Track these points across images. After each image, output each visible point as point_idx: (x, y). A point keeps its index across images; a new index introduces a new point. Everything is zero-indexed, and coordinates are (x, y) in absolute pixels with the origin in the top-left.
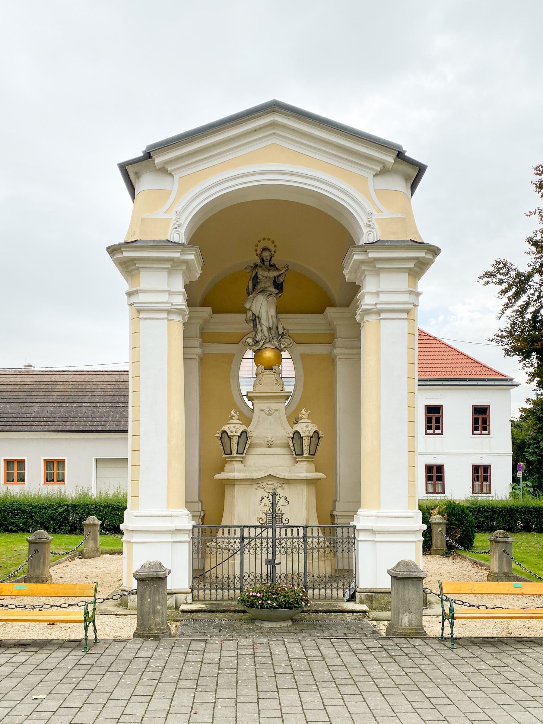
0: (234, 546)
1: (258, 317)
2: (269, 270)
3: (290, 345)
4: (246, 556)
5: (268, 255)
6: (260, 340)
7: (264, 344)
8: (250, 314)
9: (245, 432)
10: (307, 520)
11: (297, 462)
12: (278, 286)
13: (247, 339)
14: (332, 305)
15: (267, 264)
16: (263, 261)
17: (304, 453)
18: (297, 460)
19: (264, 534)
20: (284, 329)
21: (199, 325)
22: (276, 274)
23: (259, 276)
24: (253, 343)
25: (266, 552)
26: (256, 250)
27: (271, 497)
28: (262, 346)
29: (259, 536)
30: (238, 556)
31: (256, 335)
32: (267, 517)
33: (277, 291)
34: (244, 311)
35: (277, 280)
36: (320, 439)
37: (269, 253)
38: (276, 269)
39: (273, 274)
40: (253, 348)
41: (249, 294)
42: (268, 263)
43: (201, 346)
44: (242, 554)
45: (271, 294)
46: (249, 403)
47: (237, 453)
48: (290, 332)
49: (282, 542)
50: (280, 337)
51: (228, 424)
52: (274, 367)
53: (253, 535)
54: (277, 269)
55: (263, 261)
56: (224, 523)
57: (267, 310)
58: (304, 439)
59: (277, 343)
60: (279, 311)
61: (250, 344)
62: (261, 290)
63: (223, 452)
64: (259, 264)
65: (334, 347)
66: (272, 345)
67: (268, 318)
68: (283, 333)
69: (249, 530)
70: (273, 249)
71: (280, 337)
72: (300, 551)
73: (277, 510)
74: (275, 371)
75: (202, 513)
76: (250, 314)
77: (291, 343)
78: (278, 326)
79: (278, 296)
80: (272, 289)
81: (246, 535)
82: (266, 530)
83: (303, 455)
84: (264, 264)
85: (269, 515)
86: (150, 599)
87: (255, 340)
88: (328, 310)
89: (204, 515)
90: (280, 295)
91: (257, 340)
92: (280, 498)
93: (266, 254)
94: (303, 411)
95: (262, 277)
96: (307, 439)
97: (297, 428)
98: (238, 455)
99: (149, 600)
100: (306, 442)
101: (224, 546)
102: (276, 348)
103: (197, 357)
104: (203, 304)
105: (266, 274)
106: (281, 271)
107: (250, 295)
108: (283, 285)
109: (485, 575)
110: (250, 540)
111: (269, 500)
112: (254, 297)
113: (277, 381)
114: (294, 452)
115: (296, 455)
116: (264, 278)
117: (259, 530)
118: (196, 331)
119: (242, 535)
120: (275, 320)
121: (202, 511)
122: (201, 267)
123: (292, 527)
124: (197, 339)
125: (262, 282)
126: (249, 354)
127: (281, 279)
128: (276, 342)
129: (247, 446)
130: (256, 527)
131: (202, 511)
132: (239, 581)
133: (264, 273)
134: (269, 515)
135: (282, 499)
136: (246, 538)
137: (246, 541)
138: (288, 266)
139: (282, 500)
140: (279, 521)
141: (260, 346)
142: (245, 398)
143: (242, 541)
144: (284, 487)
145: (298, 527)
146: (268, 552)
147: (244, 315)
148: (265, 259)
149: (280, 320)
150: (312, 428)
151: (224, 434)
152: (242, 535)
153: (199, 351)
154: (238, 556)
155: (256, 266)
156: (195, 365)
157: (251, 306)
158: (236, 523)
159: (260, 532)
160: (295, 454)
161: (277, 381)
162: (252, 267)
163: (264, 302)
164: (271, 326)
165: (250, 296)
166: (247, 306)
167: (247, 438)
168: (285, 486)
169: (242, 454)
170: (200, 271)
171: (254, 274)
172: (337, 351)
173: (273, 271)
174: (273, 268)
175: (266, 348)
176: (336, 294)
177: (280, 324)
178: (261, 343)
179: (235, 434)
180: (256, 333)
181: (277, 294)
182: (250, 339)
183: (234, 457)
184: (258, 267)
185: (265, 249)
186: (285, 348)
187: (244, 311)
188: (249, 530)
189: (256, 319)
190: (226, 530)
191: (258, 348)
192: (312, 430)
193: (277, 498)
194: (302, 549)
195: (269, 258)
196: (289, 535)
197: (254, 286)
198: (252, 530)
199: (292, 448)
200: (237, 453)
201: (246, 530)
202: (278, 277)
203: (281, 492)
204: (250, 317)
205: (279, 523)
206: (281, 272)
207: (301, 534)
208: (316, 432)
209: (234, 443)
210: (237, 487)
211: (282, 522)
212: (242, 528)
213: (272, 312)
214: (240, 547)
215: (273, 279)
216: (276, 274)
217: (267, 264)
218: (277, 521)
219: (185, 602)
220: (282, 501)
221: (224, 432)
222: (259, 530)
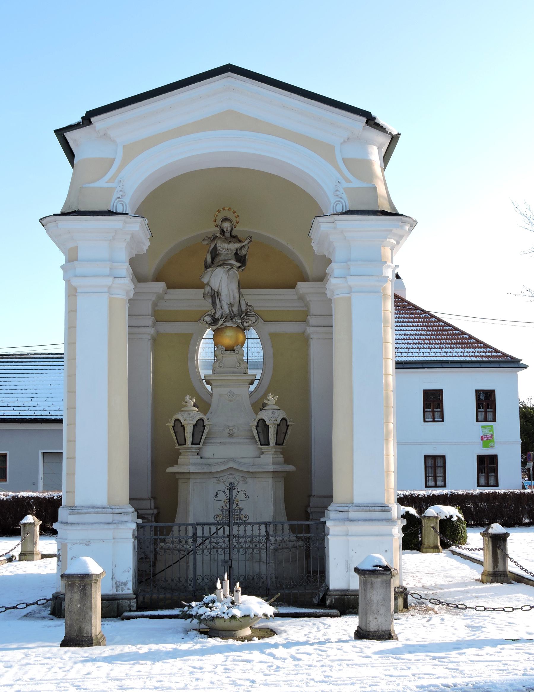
0: (185, 546)
1: (218, 293)
2: (229, 241)
3: (255, 324)
4: (199, 557)
5: (229, 226)
6: (220, 318)
7: (224, 322)
8: (208, 289)
9: (202, 420)
10: (274, 517)
11: (263, 453)
12: (241, 259)
13: (205, 316)
14: (305, 279)
15: (228, 235)
16: (223, 232)
17: (270, 443)
18: (262, 451)
19: (221, 532)
20: (247, 305)
21: (151, 302)
22: (237, 245)
23: (219, 248)
24: (212, 321)
25: (223, 552)
26: (215, 221)
27: (227, 492)
28: (222, 325)
29: (215, 535)
30: (191, 557)
31: (215, 312)
32: (223, 514)
33: (238, 264)
34: (202, 286)
35: (239, 253)
36: (289, 427)
37: (230, 224)
38: (237, 241)
39: (234, 246)
40: (211, 326)
41: (207, 267)
42: (229, 234)
43: (154, 325)
44: (195, 554)
45: (232, 268)
46: (209, 388)
47: (193, 444)
48: (255, 309)
49: (240, 541)
50: (244, 314)
51: (182, 411)
52: (235, 348)
53: (206, 534)
54: (240, 241)
55: (223, 232)
56: (178, 520)
57: (228, 286)
58: (269, 427)
59: (239, 321)
60: (241, 286)
61: (209, 323)
62: (220, 263)
63: (176, 442)
64: (218, 235)
65: (308, 325)
66: (234, 323)
67: (229, 293)
68: (246, 310)
69: (203, 528)
70: (234, 219)
71: (244, 314)
72: (262, 551)
73: (235, 505)
74: (237, 352)
75: (155, 511)
76: (208, 289)
77: (256, 321)
78: (241, 301)
79: (240, 270)
80: (233, 262)
81: (199, 533)
82: (222, 529)
83: (269, 445)
84: (224, 235)
85: (226, 512)
86: (81, 604)
87: (214, 318)
88: (300, 285)
89: (158, 513)
90: (243, 268)
91: (216, 317)
92: (238, 492)
93: (227, 225)
94: (270, 396)
95: (221, 249)
96: (273, 428)
97: (263, 415)
98: (194, 446)
99: (79, 606)
100: (272, 431)
101: (174, 546)
102: (238, 326)
103: (149, 337)
104: (157, 279)
105: (226, 246)
106: (243, 242)
107: (208, 268)
108: (247, 258)
109: (256, 566)
110: (204, 539)
111: (226, 495)
112: (213, 271)
113: (240, 364)
114: (258, 442)
115: (261, 445)
116: (224, 250)
117: (213, 528)
118: (148, 309)
119: (195, 534)
120: (237, 295)
121: (155, 508)
122: (149, 238)
123: (252, 524)
124: (149, 317)
125: (222, 254)
126: (209, 333)
127: (244, 252)
128: (238, 319)
129: (204, 436)
130: (210, 524)
131: (155, 508)
132: (192, 585)
133: (224, 244)
134: (226, 512)
135: (241, 493)
136: (200, 537)
137: (199, 541)
138: (251, 238)
139: (241, 493)
140: (237, 518)
141: (219, 325)
142: (204, 381)
143: (195, 540)
144: (247, 481)
145: (259, 524)
146: (224, 552)
147: (201, 291)
148: (225, 230)
149: (243, 296)
150: (280, 415)
151: (177, 422)
152: (195, 534)
153: (152, 331)
154: (191, 557)
155: (215, 238)
156: (146, 347)
157: (209, 281)
158: (191, 520)
159: (219, 532)
160: (260, 445)
161: (240, 364)
162: (210, 238)
163: (225, 277)
164: (232, 302)
165: (208, 270)
166: (205, 280)
167: (204, 426)
168: (249, 480)
169: (199, 444)
170: (148, 243)
171: (212, 246)
172: (310, 330)
173: (234, 243)
174: (235, 239)
175: (227, 327)
176: (310, 269)
177: (243, 301)
178: (221, 322)
179: (190, 422)
180: (215, 310)
181: (239, 267)
182: (208, 316)
183: (188, 448)
184: (217, 239)
185: (225, 220)
186: (248, 326)
187: (202, 286)
188: (203, 528)
189: (215, 296)
190: (183, 528)
191: (217, 326)
192: (279, 418)
193: (235, 492)
194: (263, 549)
195: (229, 229)
196: (249, 533)
197: (213, 259)
198: (206, 528)
199: (257, 437)
200: (193, 444)
201: (199, 528)
202: (241, 248)
203: (240, 487)
204: (208, 293)
205: (237, 520)
206: (243, 244)
207: (263, 532)
208: (283, 419)
209: (188, 433)
210: (192, 481)
211: (240, 519)
212: (195, 526)
213: (234, 286)
214: (192, 547)
215: (235, 251)
216: (237, 245)
217: (228, 235)
218: (234, 518)
219: (129, 609)
220: (241, 496)
221: (177, 420)
222: (213, 528)
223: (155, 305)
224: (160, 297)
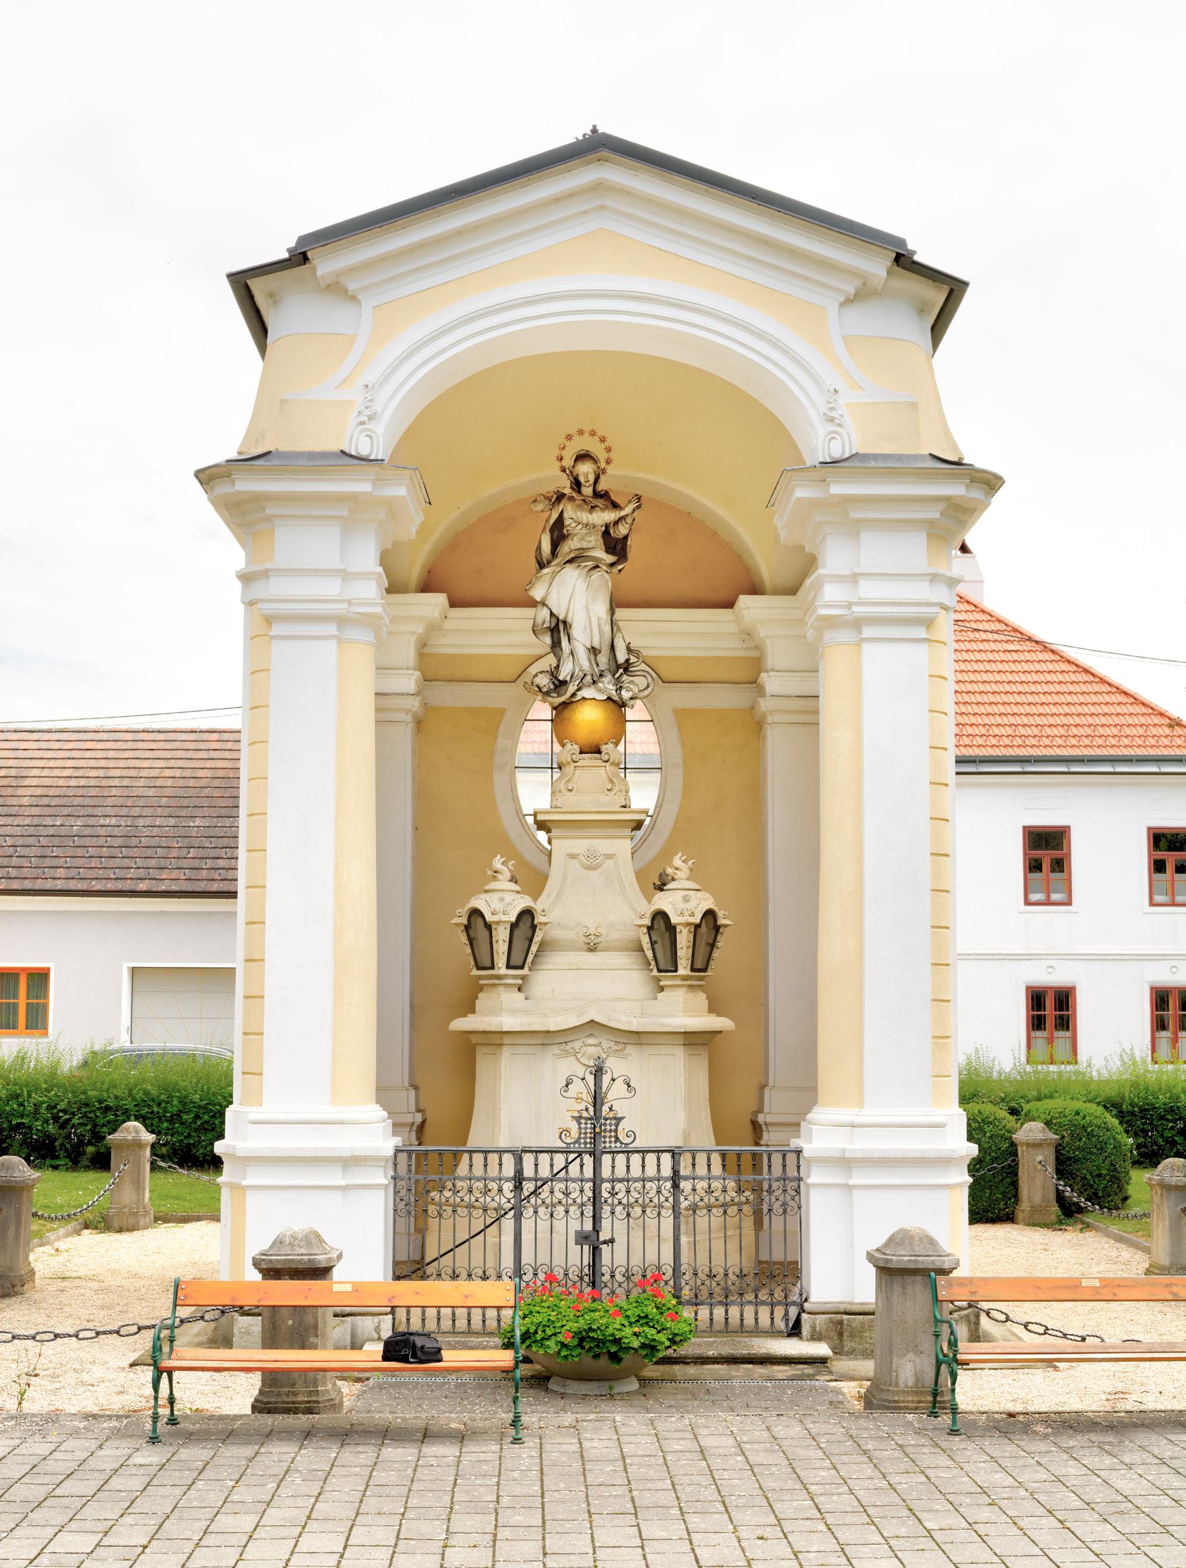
0: (497, 1198)
1: (565, 622)
2: (592, 507)
3: (646, 692)
4: (527, 1224)
5: (591, 470)
9: (528, 914)
10: (687, 1135)
11: (662, 989)
12: (616, 547)
13: (536, 675)
15: (587, 491)
16: (577, 484)
17: (680, 967)
19: (574, 1169)
20: (629, 650)
21: (414, 638)
22: (610, 516)
23: (567, 522)
24: (552, 687)
25: (579, 1213)
26: (561, 459)
27: (590, 1079)
28: (574, 695)
29: (563, 1174)
30: (508, 1223)
33: (611, 559)
35: (612, 531)
36: (721, 930)
38: (609, 504)
40: (550, 699)
41: (542, 565)
42: (591, 488)
44: (518, 1218)
45: (597, 567)
46: (542, 836)
47: (509, 967)
49: (616, 1190)
51: (486, 891)
52: (603, 748)
53: (545, 1172)
54: (615, 506)
55: (577, 484)
56: (473, 1142)
58: (678, 930)
61: (545, 690)
62: (572, 555)
63: (473, 963)
64: (567, 491)
67: (590, 624)
68: (627, 661)
69: (536, 1159)
70: (602, 456)
71: (621, 671)
72: (663, 1212)
73: (605, 1108)
74: (606, 757)
75: (418, 1118)
76: (543, 614)
77: (648, 686)
78: (615, 643)
79: (615, 570)
80: (601, 554)
81: (528, 1172)
83: (676, 970)
84: (580, 492)
85: (586, 1124)
87: (556, 678)
89: (423, 1123)
90: (620, 567)
91: (561, 678)
92: (613, 1080)
93: (585, 470)
94: (677, 861)
95: (574, 525)
96: (685, 931)
97: (663, 901)
100: (684, 939)
102: (609, 698)
103: (409, 718)
105: (585, 516)
108: (629, 542)
110: (539, 1183)
114: (653, 963)
115: (659, 971)
116: (580, 527)
117: (560, 1160)
118: (408, 654)
120: (607, 629)
123: (644, 1152)
126: (542, 710)
127: (622, 530)
129: (534, 948)
130: (552, 1152)
131: (419, 1110)
133: (579, 513)
134: (586, 1124)
135: (619, 1082)
136: (529, 1179)
137: (528, 1187)
138: (639, 499)
139: (619, 1083)
140: (610, 1137)
143: (518, 1187)
144: (626, 1051)
146: (582, 1214)
148: (582, 479)
150: (702, 902)
153: (415, 704)
154: (508, 1223)
158: (503, 1144)
159: (563, 1164)
160: (655, 970)
161: (612, 782)
162: (549, 499)
164: (596, 645)
165: (545, 571)
166: (537, 593)
167: (534, 927)
168: (630, 1050)
169: (522, 967)
171: (555, 516)
173: (603, 510)
175: (584, 698)
177: (621, 641)
178: (572, 689)
179: (504, 918)
180: (559, 661)
181: (612, 565)
183: (499, 977)
184: (564, 501)
185: (583, 457)
186: (632, 698)
188: (536, 1159)
189: (558, 629)
193: (606, 1079)
194: (667, 1209)
195: (592, 478)
196: (636, 1172)
197: (555, 546)
198: (544, 1159)
199: (649, 954)
200: (509, 967)
202: (616, 523)
203: (615, 1066)
204: (544, 622)
205: (610, 1142)
206: (623, 513)
207: (667, 1171)
208: (710, 914)
209: (501, 942)
210: (506, 1052)
211: (617, 1139)
213: (601, 608)
214: (512, 1201)
215: (603, 529)
216: (610, 516)
217: (587, 491)
218: (605, 1137)
219: (376, 1336)
220: (619, 1086)
221: (476, 913)
222: (560, 1160)
223: (422, 645)
224: (433, 628)
